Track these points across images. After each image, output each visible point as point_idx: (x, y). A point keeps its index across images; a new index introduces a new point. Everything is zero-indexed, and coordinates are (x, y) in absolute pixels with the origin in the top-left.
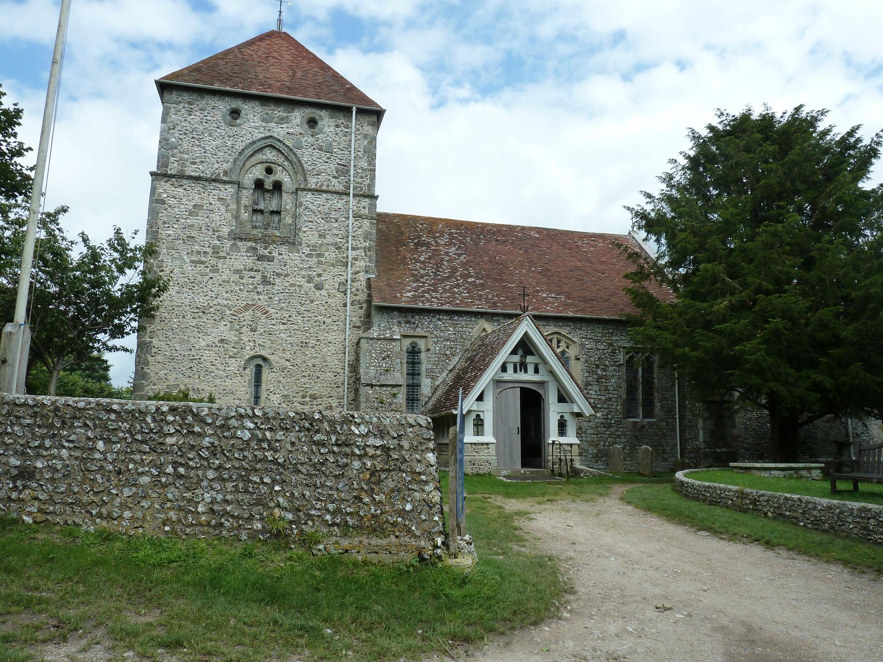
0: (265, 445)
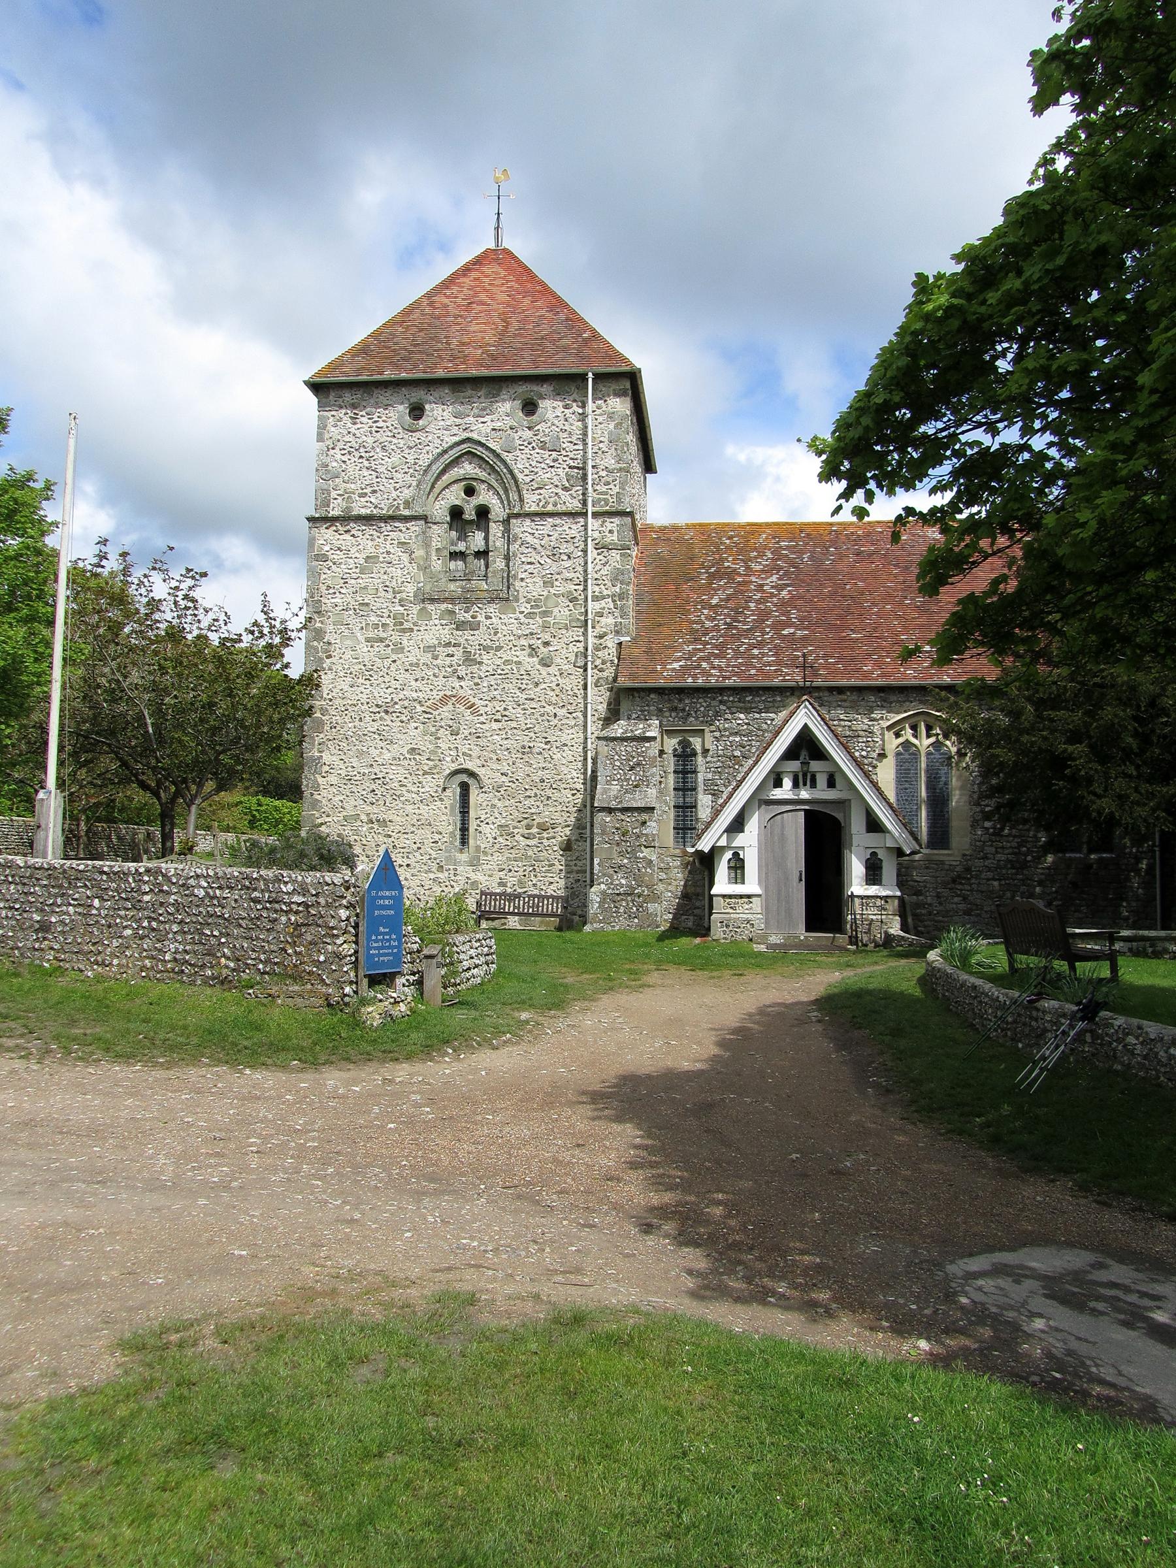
0: (215, 902)
